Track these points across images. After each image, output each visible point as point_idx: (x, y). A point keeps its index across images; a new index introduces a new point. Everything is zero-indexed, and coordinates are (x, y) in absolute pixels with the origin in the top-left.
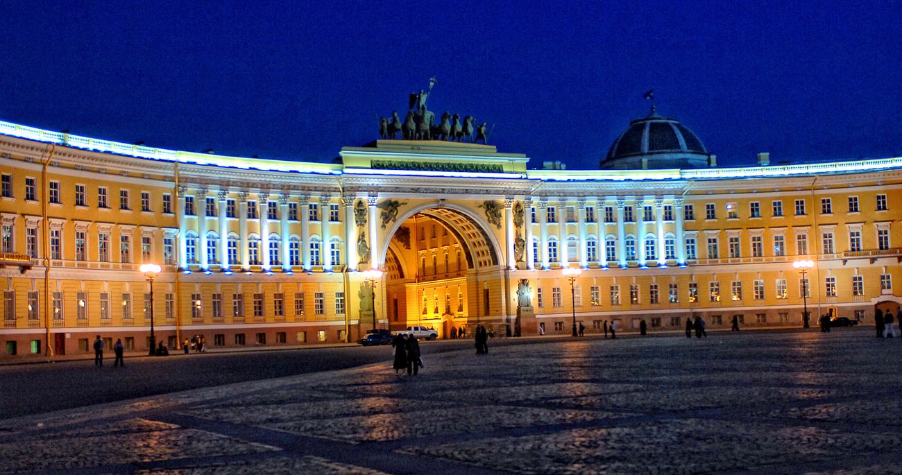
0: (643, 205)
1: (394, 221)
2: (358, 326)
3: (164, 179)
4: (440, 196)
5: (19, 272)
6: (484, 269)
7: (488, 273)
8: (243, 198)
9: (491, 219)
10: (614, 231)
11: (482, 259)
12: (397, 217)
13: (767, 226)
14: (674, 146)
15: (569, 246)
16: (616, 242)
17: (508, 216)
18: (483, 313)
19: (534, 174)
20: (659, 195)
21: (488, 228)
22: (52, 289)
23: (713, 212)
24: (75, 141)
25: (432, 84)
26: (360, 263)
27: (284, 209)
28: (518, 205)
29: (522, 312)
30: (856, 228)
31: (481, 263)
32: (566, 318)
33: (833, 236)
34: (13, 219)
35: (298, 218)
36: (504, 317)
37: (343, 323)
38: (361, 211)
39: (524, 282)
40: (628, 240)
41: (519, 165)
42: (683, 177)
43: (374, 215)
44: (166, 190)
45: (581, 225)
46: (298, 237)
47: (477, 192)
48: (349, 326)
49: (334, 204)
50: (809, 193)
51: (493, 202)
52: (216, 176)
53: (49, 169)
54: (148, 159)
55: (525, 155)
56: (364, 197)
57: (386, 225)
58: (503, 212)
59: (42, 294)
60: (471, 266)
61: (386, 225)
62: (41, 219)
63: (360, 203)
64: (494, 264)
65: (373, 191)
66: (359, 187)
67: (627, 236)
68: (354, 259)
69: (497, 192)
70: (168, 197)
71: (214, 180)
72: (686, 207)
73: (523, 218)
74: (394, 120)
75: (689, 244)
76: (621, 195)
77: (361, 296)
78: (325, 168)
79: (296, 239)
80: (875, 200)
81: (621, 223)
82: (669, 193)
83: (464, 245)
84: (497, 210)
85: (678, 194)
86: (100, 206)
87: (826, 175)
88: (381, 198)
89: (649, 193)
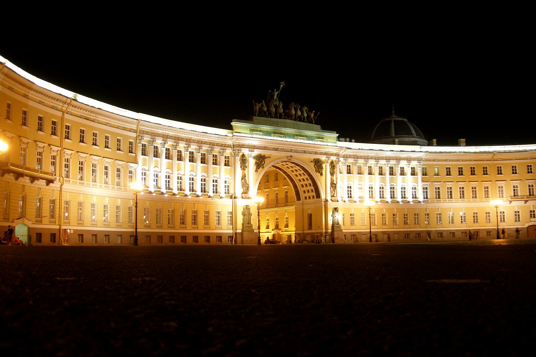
0: (400, 166)
1: (263, 168)
2: (242, 233)
3: (130, 130)
4: (290, 154)
5: (45, 184)
6: (308, 201)
7: (313, 203)
8: (175, 147)
10: (384, 181)
11: (307, 195)
13: (480, 181)
14: (409, 134)
15: (359, 189)
17: (326, 168)
18: (307, 228)
20: (409, 160)
21: (316, 175)
22: (64, 199)
23: (449, 171)
24: (82, 99)
26: (242, 193)
27: (198, 157)
28: (332, 162)
30: (516, 183)
31: (306, 198)
33: (504, 187)
34: (44, 147)
35: (206, 162)
36: (324, 231)
37: (231, 231)
38: (244, 161)
39: (336, 209)
43: (252, 163)
44: (131, 137)
45: (366, 176)
46: (206, 175)
48: (236, 233)
49: (227, 155)
50: (490, 162)
51: (319, 159)
53: (67, 116)
56: (246, 151)
58: (324, 166)
59: (58, 201)
60: (299, 199)
62: (60, 149)
63: (243, 156)
64: (317, 198)
65: (252, 148)
68: (239, 191)
69: (321, 154)
70: (132, 142)
72: (423, 168)
76: (388, 159)
77: (244, 214)
78: (223, 132)
79: (204, 176)
80: (526, 168)
81: (388, 176)
82: (414, 159)
83: (295, 186)
85: (419, 160)
86: (93, 144)
87: (499, 152)
88: (256, 152)
89: (403, 159)
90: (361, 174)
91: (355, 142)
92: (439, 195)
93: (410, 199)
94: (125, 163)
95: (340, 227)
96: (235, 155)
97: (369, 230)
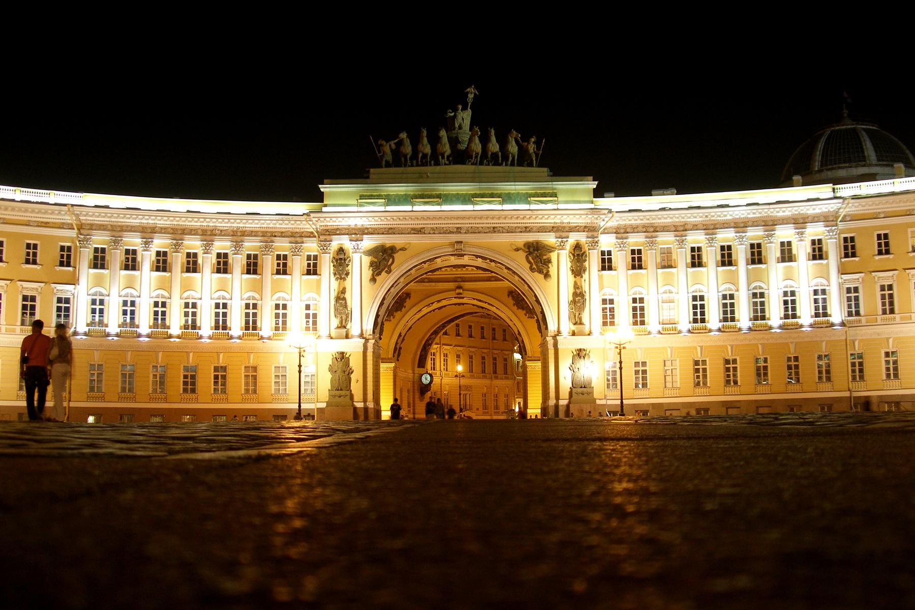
1: (389, 272)
3: (61, 226)
9: (534, 266)
12: (392, 267)
14: (859, 158)
16: (736, 294)
17: (561, 262)
19: (610, 202)
20: (800, 222)
21: (534, 280)
25: (471, 96)
27: (238, 262)
28: (577, 247)
29: (574, 394)
32: (653, 404)
35: (259, 272)
40: (755, 291)
41: (585, 191)
42: (838, 195)
43: (359, 265)
47: (510, 231)
49: (312, 254)
51: (537, 242)
52: (135, 222)
54: (37, 203)
55: (591, 178)
56: (345, 242)
57: (377, 278)
58: (553, 256)
61: (377, 278)
63: (341, 250)
66: (338, 229)
67: (753, 285)
69: (542, 229)
71: (132, 227)
72: (845, 239)
73: (586, 264)
74: (400, 144)
75: (852, 297)
76: (740, 226)
79: (254, 298)
82: (815, 219)
84: (541, 255)
85: (829, 220)
88: (369, 242)
89: (784, 221)
90: (670, 267)
91: (615, 197)
92: (892, 304)
93: (806, 316)
94: (42, 285)
95: (591, 393)
96: (296, 252)
97: (619, 402)
